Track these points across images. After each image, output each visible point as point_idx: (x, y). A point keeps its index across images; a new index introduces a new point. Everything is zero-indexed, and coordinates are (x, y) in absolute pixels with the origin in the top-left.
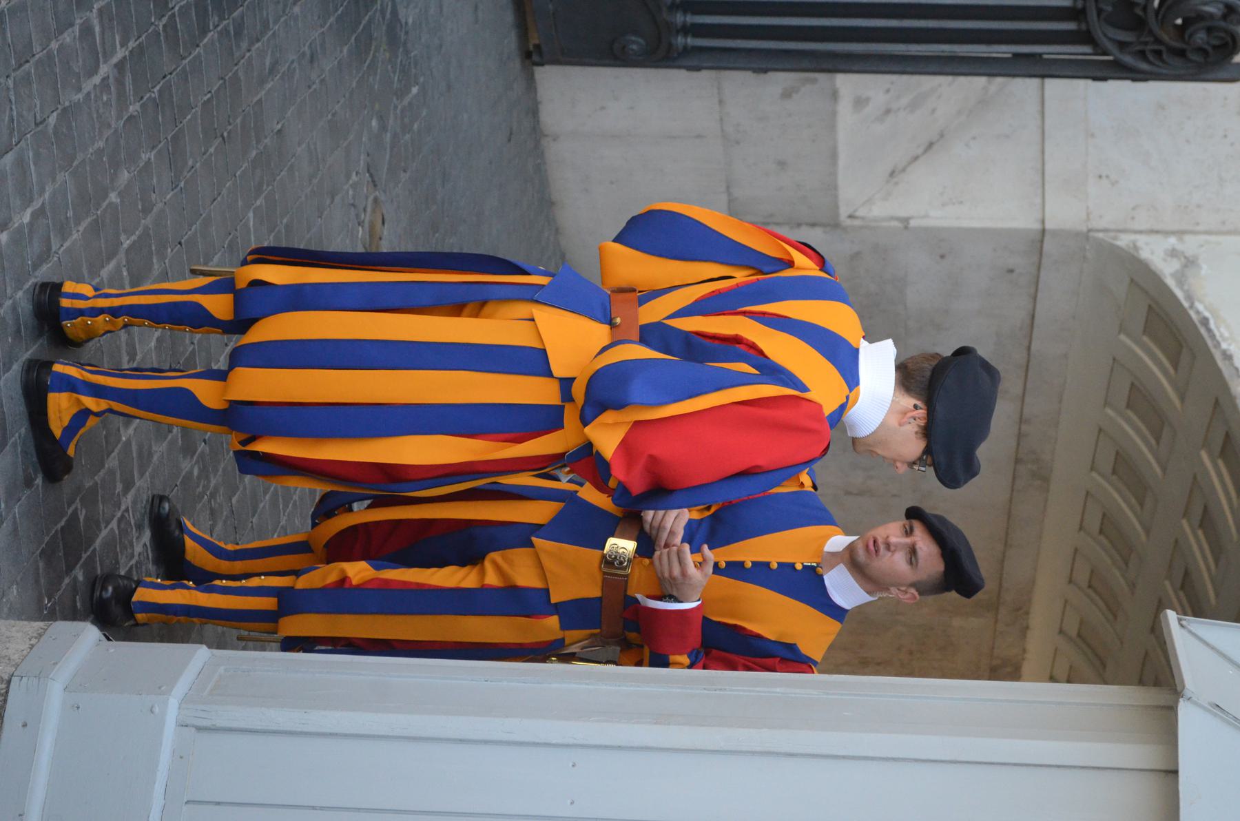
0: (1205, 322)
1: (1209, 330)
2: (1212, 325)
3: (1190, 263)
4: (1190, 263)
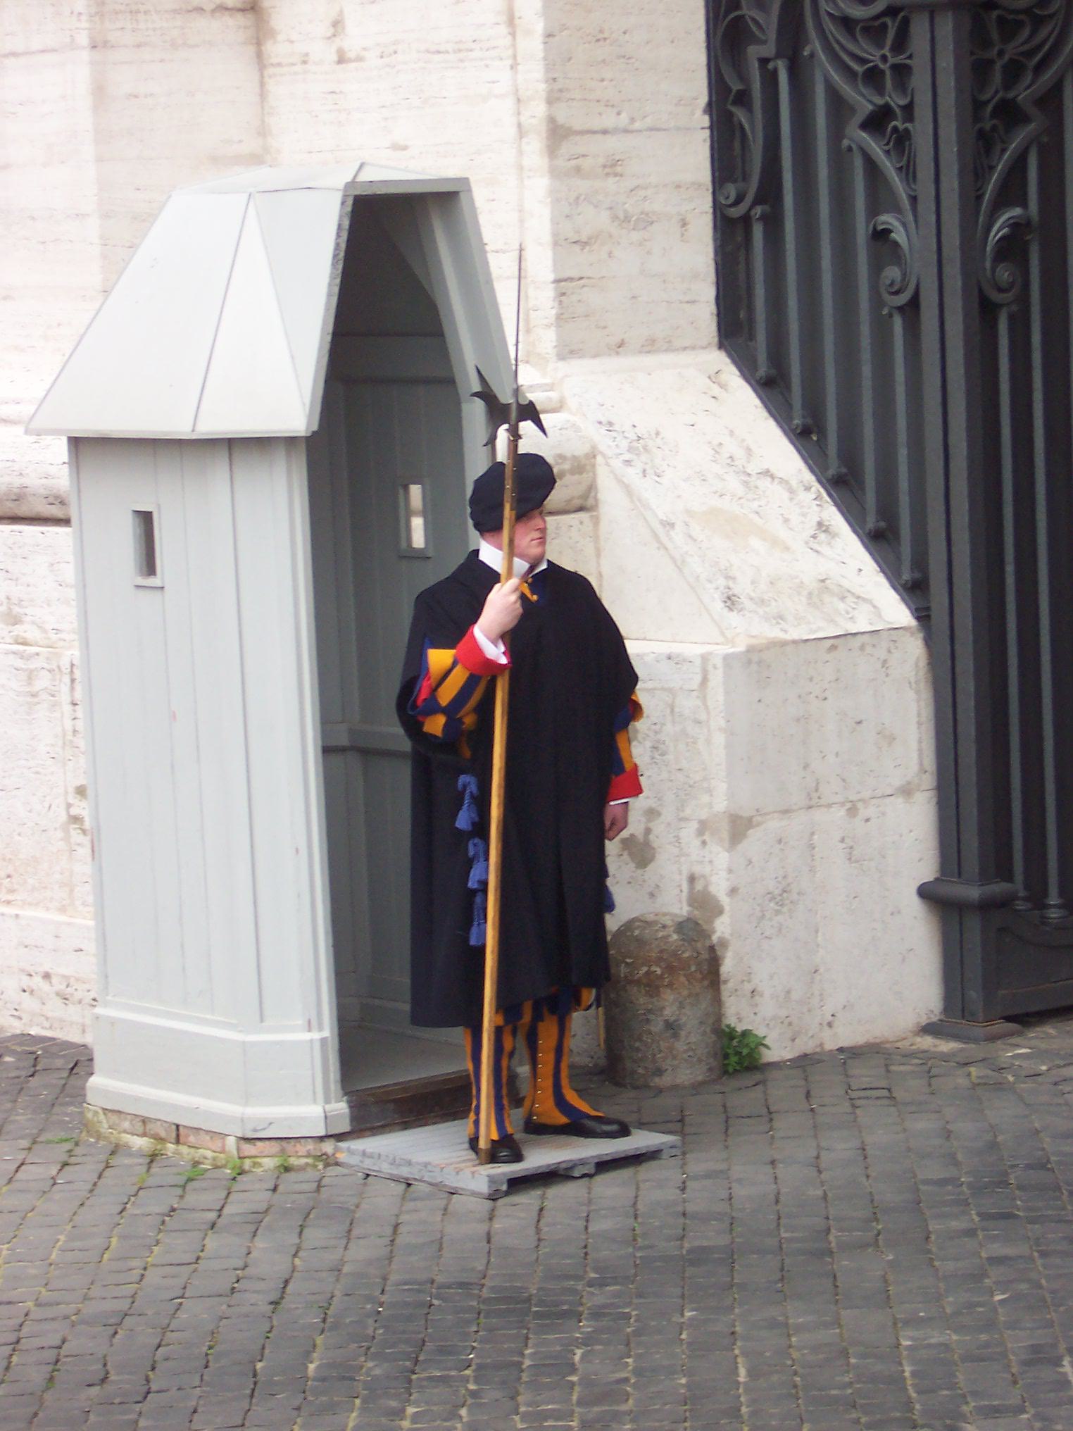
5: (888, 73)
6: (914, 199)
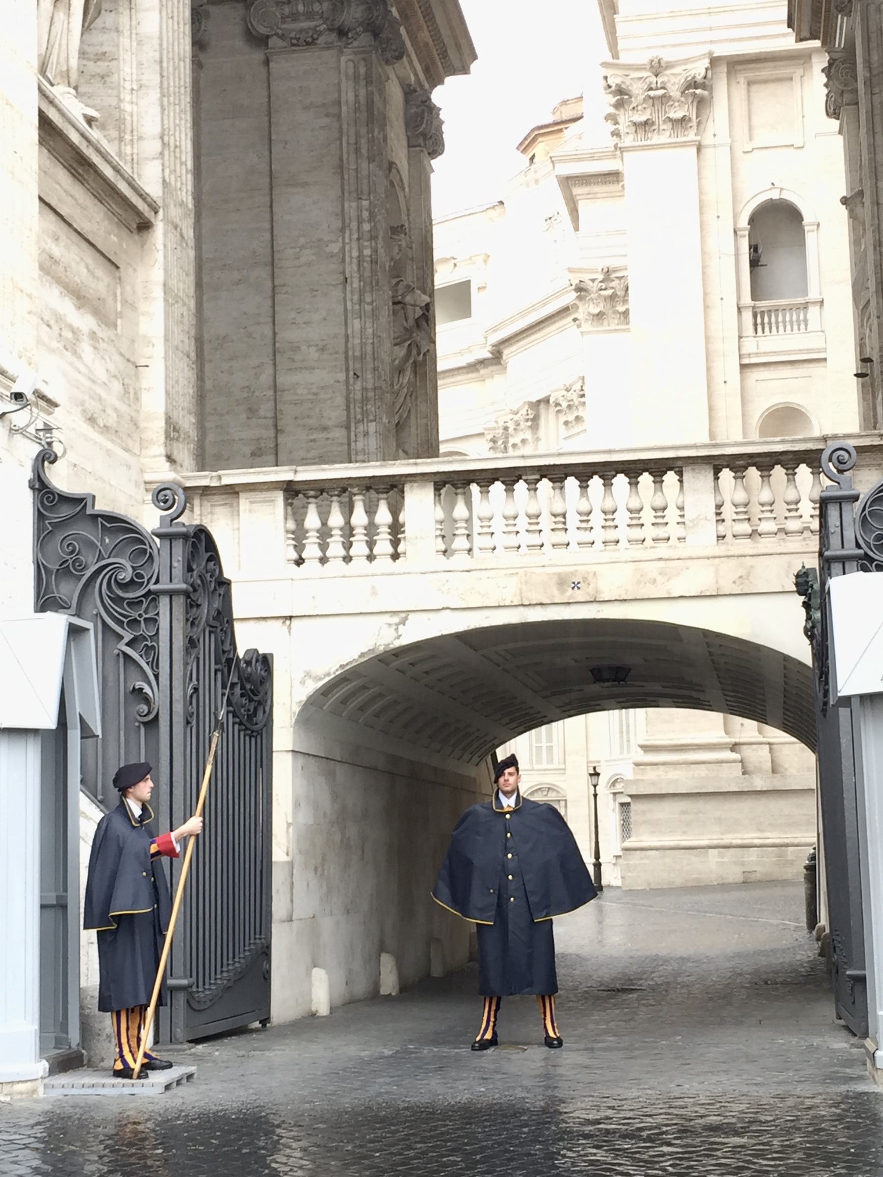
0: (342, 666)
1: (347, 664)
2: (345, 663)
3: (308, 675)
4: (308, 675)
5: (142, 622)
6: (157, 676)
